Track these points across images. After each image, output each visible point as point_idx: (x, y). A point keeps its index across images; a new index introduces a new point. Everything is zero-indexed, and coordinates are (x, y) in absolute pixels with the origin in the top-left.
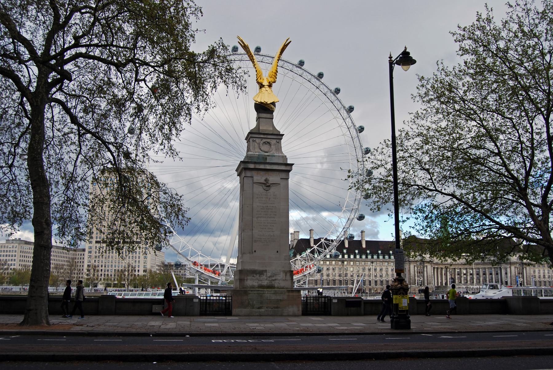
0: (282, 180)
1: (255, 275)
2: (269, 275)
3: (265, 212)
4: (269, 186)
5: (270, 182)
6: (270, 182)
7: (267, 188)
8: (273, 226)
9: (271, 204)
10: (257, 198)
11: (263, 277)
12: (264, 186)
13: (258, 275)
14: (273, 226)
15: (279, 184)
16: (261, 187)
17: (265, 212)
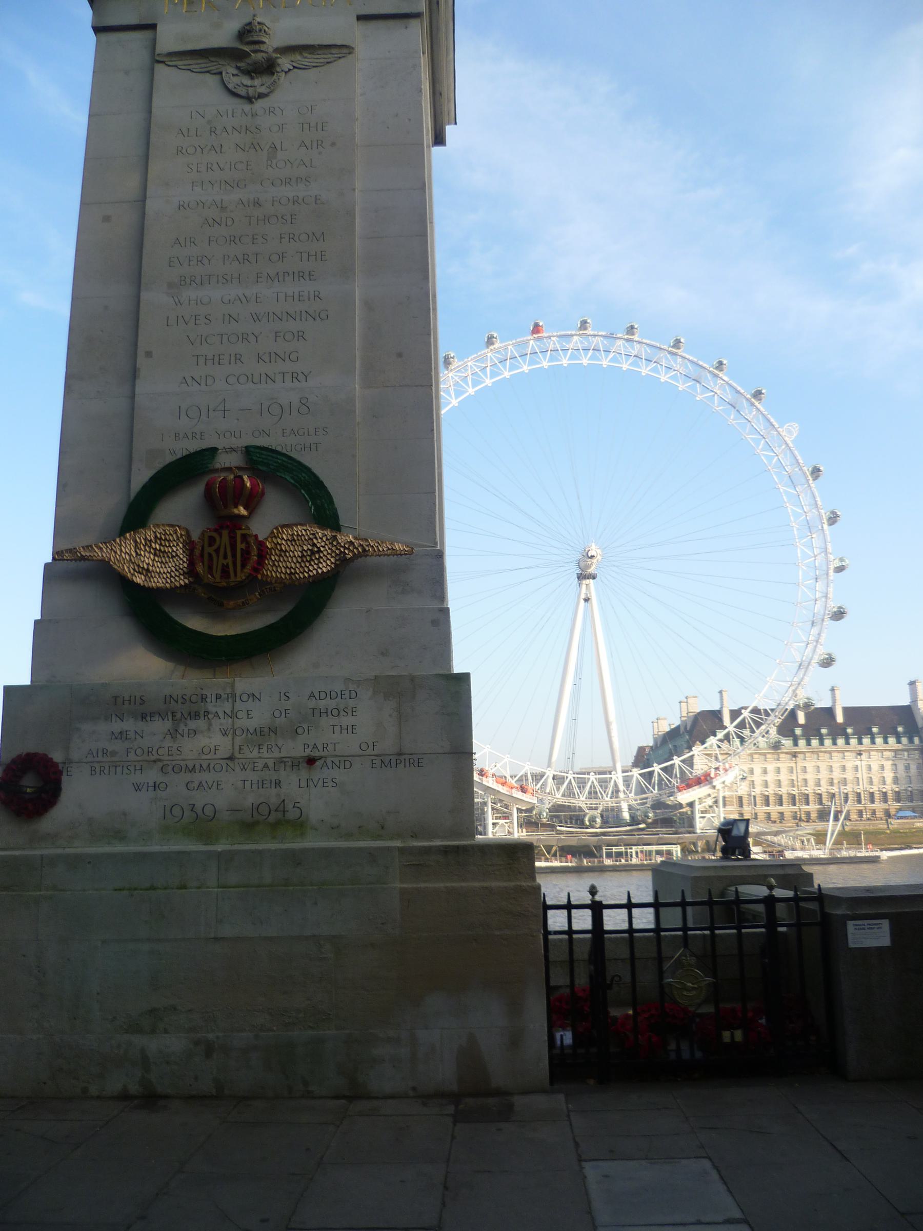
0: (373, 24)
1: (129, 725)
2: (252, 724)
3: (233, 240)
4: (268, 68)
5: (272, 42)
6: (272, 42)
7: (259, 84)
8: (300, 336)
9: (287, 181)
10: (179, 151)
11: (203, 741)
12: (229, 70)
13: (160, 726)
14: (300, 336)
15: (346, 49)
16: (212, 81)
17: (233, 240)
